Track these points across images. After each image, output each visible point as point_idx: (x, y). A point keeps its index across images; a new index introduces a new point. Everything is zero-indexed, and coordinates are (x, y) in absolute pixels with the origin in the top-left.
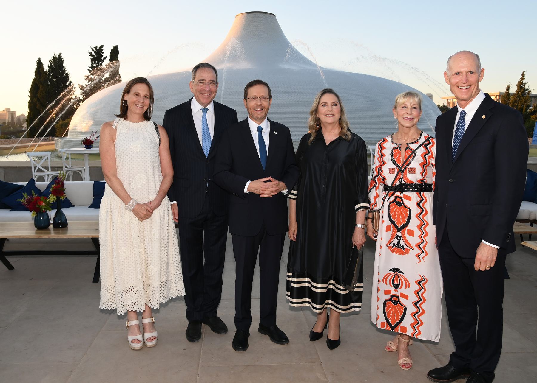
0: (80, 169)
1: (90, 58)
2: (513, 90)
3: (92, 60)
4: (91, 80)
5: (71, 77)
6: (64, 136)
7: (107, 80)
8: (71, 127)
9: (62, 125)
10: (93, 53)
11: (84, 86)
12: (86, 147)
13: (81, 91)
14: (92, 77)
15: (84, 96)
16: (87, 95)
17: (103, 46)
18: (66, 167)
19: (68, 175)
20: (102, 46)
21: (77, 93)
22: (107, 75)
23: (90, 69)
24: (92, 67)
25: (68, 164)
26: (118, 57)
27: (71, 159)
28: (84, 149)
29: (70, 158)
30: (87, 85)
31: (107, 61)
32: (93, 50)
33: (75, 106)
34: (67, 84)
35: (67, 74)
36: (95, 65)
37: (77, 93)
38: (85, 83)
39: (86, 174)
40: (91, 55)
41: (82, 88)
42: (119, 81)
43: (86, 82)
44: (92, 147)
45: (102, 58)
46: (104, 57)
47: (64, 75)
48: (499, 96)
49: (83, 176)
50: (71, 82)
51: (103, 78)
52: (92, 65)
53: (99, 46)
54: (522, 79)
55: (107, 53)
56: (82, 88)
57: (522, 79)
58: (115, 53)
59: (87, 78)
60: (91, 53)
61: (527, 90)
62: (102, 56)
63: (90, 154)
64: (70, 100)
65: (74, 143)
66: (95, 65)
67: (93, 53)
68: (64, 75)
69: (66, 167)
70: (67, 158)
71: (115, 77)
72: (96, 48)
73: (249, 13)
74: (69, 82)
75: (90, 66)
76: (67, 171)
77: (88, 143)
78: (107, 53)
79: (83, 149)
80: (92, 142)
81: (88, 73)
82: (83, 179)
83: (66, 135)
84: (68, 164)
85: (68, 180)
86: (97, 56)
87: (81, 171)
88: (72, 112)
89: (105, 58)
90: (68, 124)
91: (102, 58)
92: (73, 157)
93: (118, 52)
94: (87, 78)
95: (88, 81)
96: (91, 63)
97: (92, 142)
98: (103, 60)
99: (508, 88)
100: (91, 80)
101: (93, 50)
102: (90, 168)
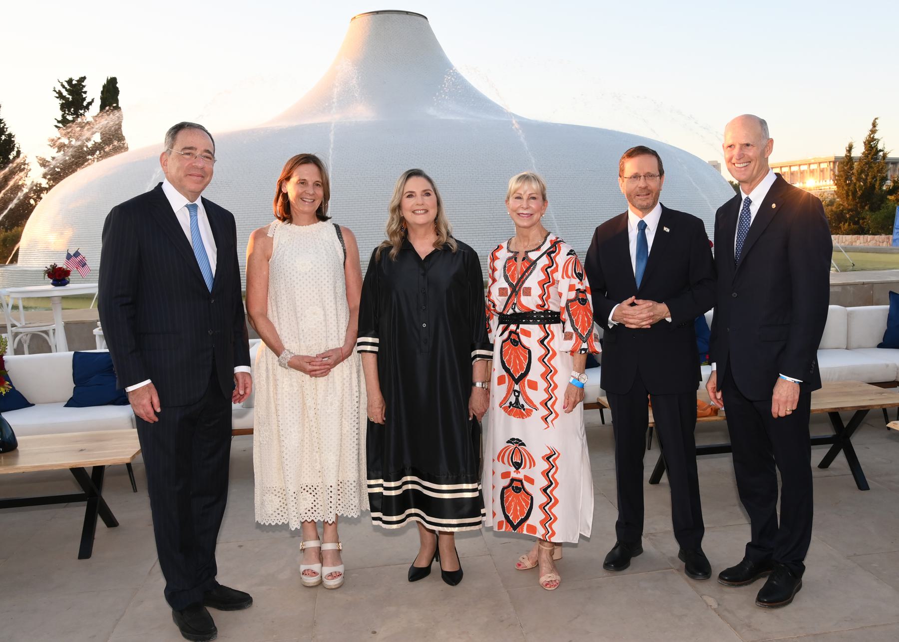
0: (44, 329)
1: (59, 102)
2: (859, 151)
3: (63, 107)
4: (61, 147)
5: (18, 141)
6: (12, 262)
7: (97, 147)
8: (23, 244)
9: (5, 240)
10: (65, 93)
11: (49, 159)
12: (56, 284)
13: (43, 170)
14: (65, 141)
15: (49, 180)
16: (56, 176)
17: (83, 79)
18: (13, 326)
19: (20, 341)
20: (83, 79)
21: (35, 176)
22: (97, 138)
23: (60, 125)
24: (64, 121)
25: (19, 320)
26: (117, 101)
27: (24, 307)
28: (51, 287)
29: (21, 307)
30: (53, 158)
31: (95, 108)
32: (63, 87)
33: (32, 202)
34: (11, 157)
35: (10, 136)
36: (70, 118)
37: (35, 176)
38: (51, 153)
39: (59, 339)
40: (60, 96)
41: (44, 163)
42: (121, 148)
43: (53, 152)
44: (68, 283)
45: (85, 104)
46: (88, 100)
47: (3, 137)
48: (834, 163)
49: (51, 341)
50: (19, 153)
51: (90, 144)
52: (63, 116)
53: (76, 78)
54: (873, 131)
55: (93, 92)
56: (44, 163)
57: (873, 131)
58: (110, 92)
59: (53, 143)
60: (60, 93)
61: (881, 151)
62: (84, 99)
63: (64, 298)
64: (17, 188)
65: (28, 277)
66: (70, 118)
67: (65, 93)
68: (3, 137)
69: (13, 326)
70: (15, 307)
71: (113, 141)
72: (70, 82)
73: (377, 12)
74: (14, 153)
75: (60, 118)
76: (16, 335)
77: (58, 276)
78: (93, 92)
79: (48, 288)
80: (67, 273)
81: (56, 133)
82: (53, 348)
83: (15, 260)
84: (19, 320)
85: (18, 351)
86: (73, 99)
87: (46, 332)
88: (23, 212)
89: (90, 104)
90: (17, 239)
91: (85, 104)
92: (26, 304)
93: (116, 91)
94: (53, 143)
95: (56, 149)
96: (61, 113)
97: (67, 273)
98: (87, 107)
99: (850, 148)
100: (61, 147)
101: (63, 87)
102: (68, 326)
